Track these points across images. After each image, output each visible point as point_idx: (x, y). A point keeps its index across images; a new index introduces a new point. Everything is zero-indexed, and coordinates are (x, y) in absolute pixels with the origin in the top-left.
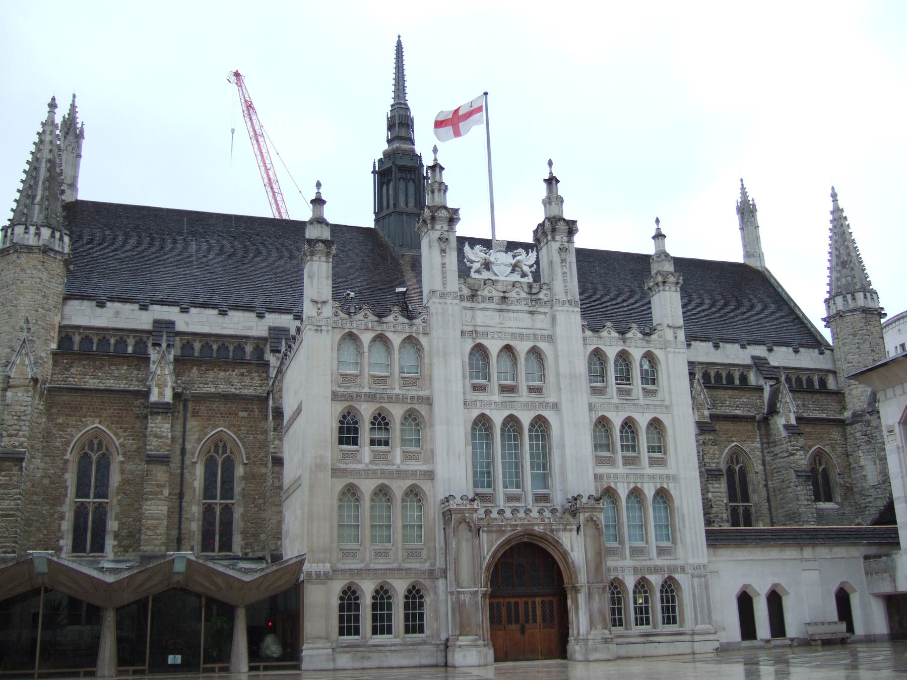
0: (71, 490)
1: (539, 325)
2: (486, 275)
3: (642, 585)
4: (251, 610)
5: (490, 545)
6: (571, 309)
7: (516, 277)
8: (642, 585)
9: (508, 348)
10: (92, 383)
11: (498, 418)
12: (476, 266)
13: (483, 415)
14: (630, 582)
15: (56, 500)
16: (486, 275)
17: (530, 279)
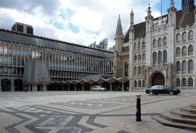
0: (124, 69)
1: (166, 32)
2: (157, 25)
3: (184, 79)
4: (123, 83)
5: (151, 73)
6: (171, 27)
7: (163, 24)
8: (184, 79)
9: (160, 38)
10: (125, 54)
11: (157, 52)
12: (155, 24)
13: (155, 52)
14: (181, 79)
15: (122, 70)
16: (157, 25)
17: (165, 23)
